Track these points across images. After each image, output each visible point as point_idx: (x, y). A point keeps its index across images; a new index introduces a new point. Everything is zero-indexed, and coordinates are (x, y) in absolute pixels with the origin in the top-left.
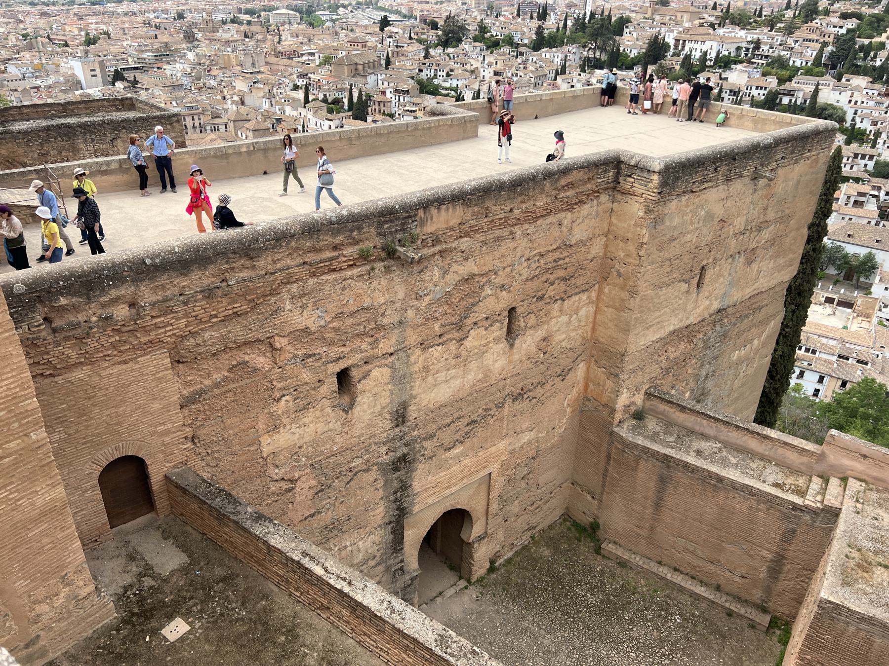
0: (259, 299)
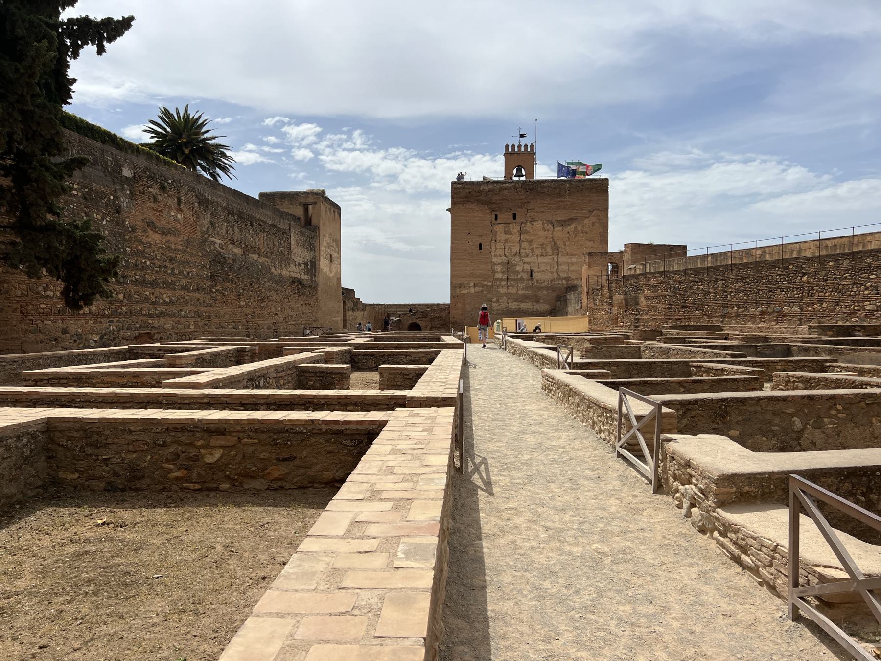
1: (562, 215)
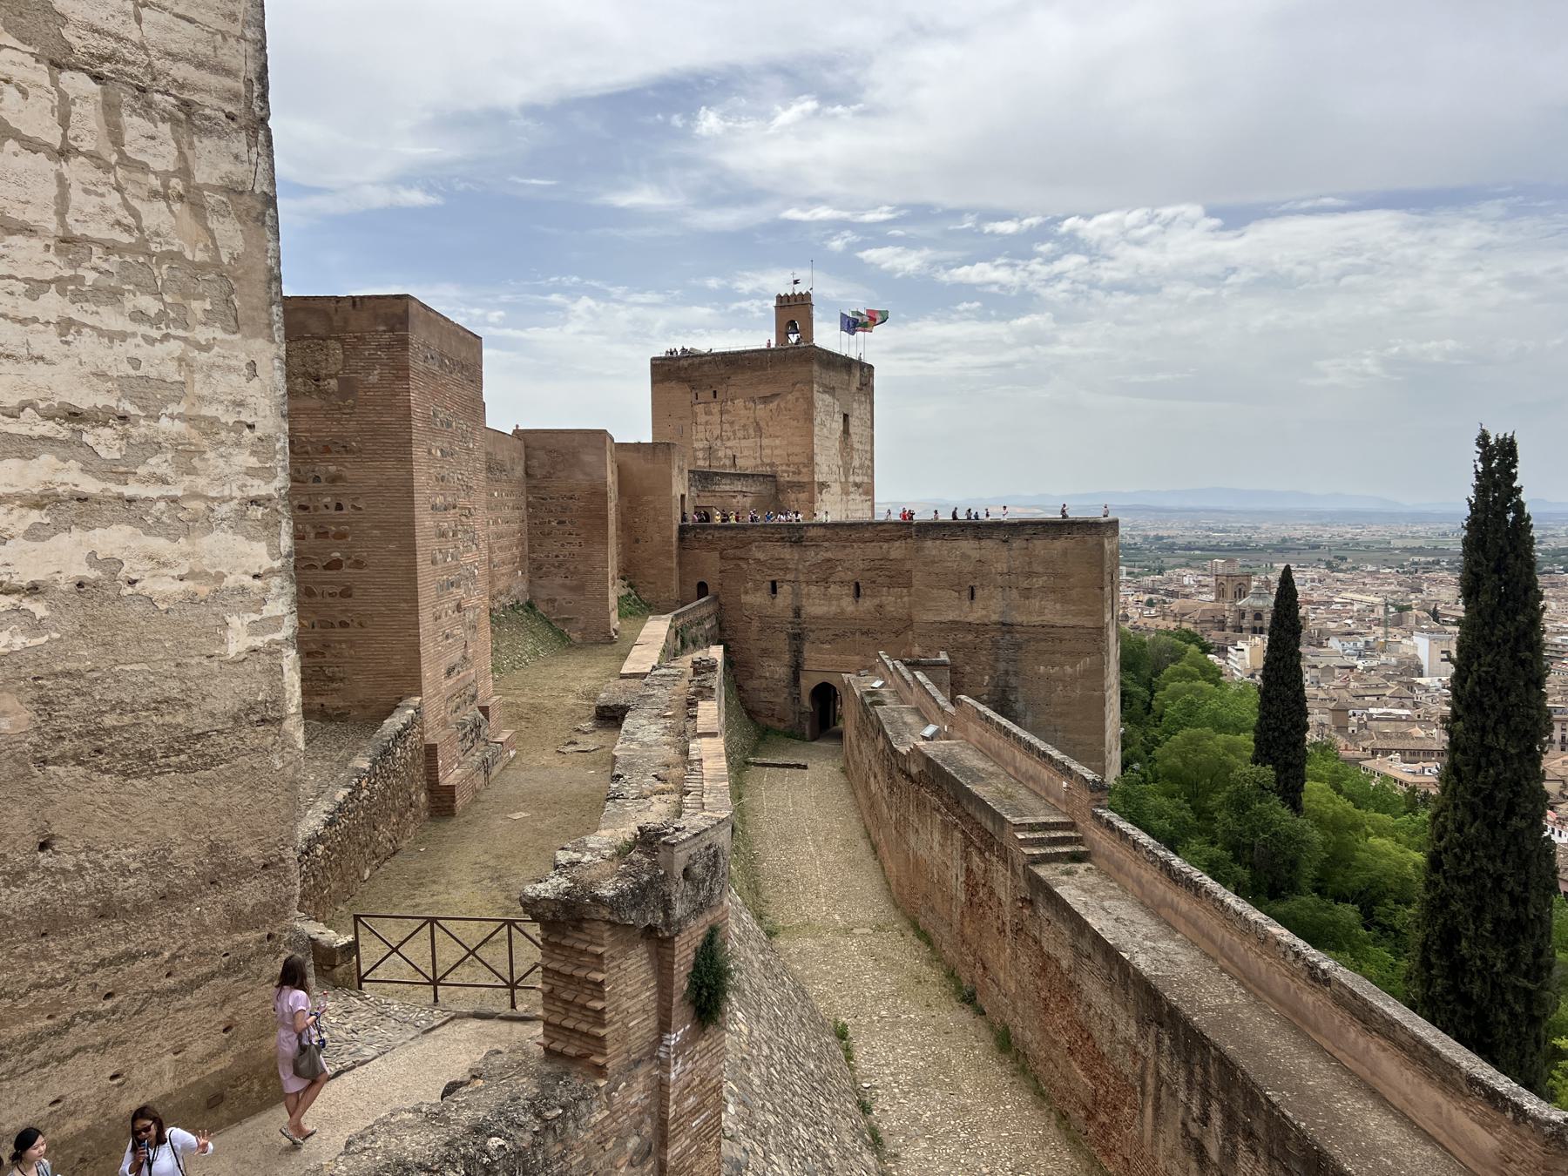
0: (746, 544)
1: (765, 391)
